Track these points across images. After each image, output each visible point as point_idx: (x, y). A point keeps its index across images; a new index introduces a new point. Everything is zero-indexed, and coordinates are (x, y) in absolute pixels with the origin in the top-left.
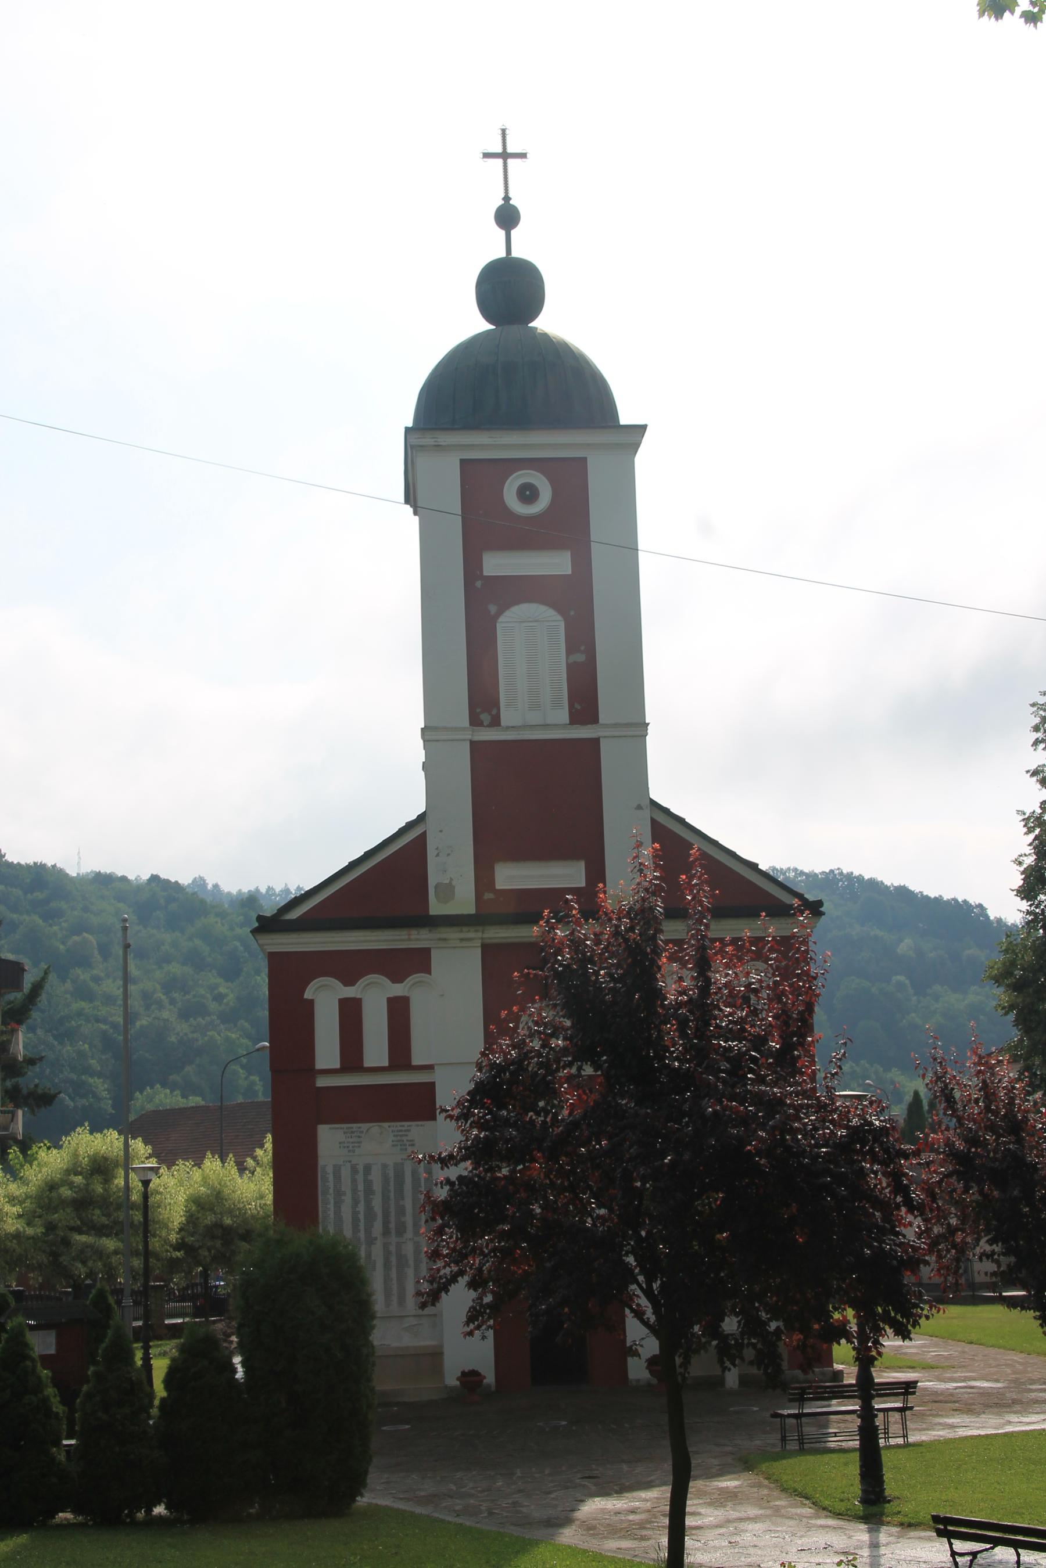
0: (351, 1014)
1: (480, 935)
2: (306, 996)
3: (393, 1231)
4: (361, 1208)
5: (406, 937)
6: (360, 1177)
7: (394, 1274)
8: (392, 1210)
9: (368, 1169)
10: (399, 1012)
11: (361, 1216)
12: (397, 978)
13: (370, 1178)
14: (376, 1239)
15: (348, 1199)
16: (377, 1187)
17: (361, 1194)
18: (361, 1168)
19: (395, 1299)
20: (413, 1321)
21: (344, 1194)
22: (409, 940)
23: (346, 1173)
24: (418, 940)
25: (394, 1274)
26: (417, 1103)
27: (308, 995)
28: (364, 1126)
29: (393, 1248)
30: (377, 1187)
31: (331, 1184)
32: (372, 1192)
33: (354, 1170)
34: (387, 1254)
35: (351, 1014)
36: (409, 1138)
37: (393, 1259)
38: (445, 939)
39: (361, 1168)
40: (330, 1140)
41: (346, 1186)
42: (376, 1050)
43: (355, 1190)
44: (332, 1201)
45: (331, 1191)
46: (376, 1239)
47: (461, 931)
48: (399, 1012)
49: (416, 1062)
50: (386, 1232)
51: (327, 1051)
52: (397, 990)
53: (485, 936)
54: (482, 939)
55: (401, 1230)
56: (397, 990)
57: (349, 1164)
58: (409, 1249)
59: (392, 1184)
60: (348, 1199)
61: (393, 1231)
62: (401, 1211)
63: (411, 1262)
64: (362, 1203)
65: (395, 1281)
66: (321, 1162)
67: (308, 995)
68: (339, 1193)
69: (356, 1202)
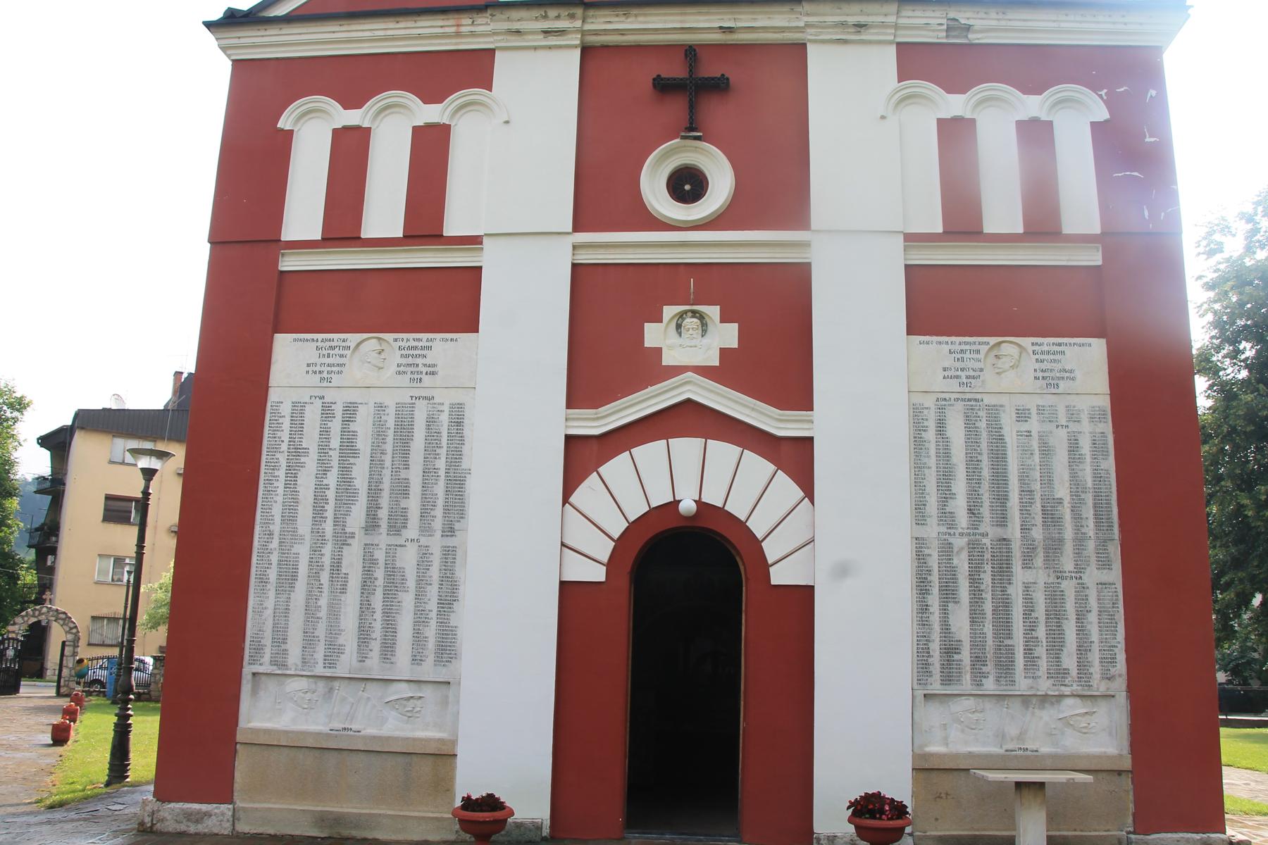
0: (350, 152)
1: (578, 24)
2: (279, 125)
3: (384, 524)
4: (332, 479)
5: (453, 29)
6: (336, 426)
7: (377, 600)
8: (386, 485)
9: (350, 411)
10: (431, 150)
11: (331, 494)
12: (432, 96)
13: (353, 427)
14: (352, 536)
15: (310, 463)
16: (364, 444)
17: (335, 455)
18: (338, 410)
19: (376, 646)
20: (404, 690)
21: (306, 454)
22: (458, 35)
23: (312, 415)
24: (473, 34)
25: (377, 600)
26: (449, 302)
27: (284, 123)
28: (353, 338)
29: (380, 555)
30: (364, 444)
31: (285, 436)
32: (355, 453)
33: (327, 412)
34: (369, 564)
35: (350, 152)
36: (427, 361)
37: (380, 574)
38: (518, 32)
39: (338, 410)
40: (293, 359)
41: (311, 440)
42: (384, 212)
43: (324, 450)
44: (283, 463)
45: (284, 447)
46: (352, 536)
47: (545, 17)
48: (431, 150)
49: (449, 231)
50: (372, 525)
51: (303, 213)
52: (431, 113)
53: (587, 27)
54: (584, 33)
55: (398, 524)
56: (431, 113)
57: (319, 403)
58: (408, 559)
59: (390, 439)
60: (310, 463)
61: (384, 524)
62: (402, 490)
63: (411, 583)
64: (335, 471)
65: (378, 615)
66: (273, 396)
67: (284, 123)
68: (297, 452)
69: (324, 470)
